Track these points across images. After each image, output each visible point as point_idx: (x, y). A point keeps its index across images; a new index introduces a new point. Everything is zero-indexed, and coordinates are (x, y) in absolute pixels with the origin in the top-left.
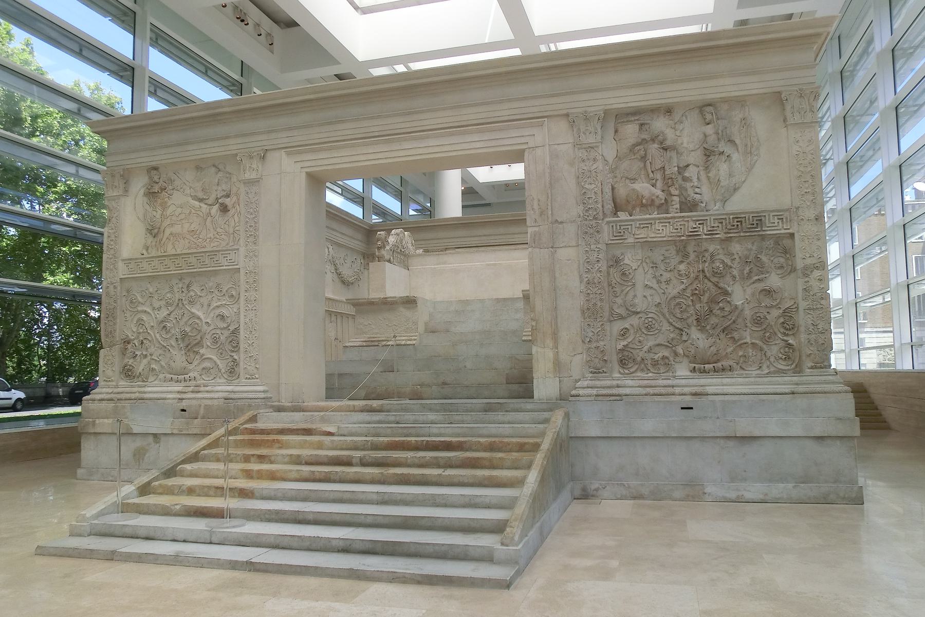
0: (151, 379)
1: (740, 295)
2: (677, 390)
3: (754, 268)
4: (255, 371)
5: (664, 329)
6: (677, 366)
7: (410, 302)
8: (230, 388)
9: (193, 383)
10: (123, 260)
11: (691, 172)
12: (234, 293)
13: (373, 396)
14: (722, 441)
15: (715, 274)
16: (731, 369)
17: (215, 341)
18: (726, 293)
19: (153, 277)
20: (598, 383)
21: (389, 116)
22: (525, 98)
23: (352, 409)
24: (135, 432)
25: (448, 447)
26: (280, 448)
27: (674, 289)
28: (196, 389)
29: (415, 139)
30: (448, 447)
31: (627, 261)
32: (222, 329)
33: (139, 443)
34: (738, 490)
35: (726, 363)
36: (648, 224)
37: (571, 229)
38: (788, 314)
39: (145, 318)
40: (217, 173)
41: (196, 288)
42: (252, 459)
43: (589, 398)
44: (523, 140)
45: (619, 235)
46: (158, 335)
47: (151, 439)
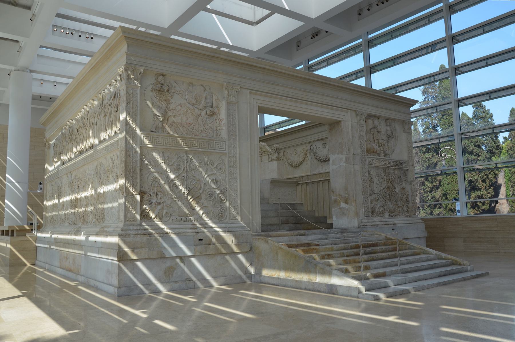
1: (397, 190)
2: (389, 223)
24: (167, 256)
33: (168, 263)
38: (407, 197)
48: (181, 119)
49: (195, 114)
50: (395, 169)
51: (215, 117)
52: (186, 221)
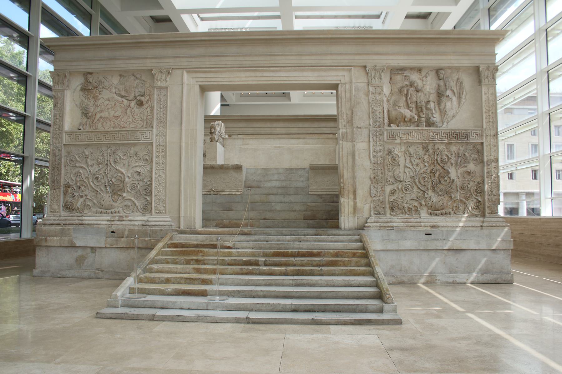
0: (86, 211)
2: (423, 224)
3: (461, 160)
4: (163, 208)
5: (414, 190)
6: (421, 211)
7: (238, 168)
8: (145, 219)
9: (118, 215)
10: (66, 132)
11: (432, 105)
12: (148, 158)
13: (221, 226)
14: (446, 252)
15: (442, 161)
16: (450, 214)
17: (133, 188)
18: (448, 172)
19: (88, 145)
20: (380, 220)
21: (256, 56)
22: (341, 54)
23: (231, 233)
25: (311, 255)
26: (203, 256)
27: (421, 169)
28: (121, 219)
29: (272, 71)
30: (311, 255)
31: (396, 152)
32: (138, 181)
33: (80, 252)
34: (453, 278)
35: (447, 211)
36: (409, 133)
37: (365, 132)
39: (81, 172)
40: (135, 80)
41: (120, 153)
42: (192, 262)
43: (376, 228)
44: (338, 78)
45: (392, 137)
46: (91, 183)
47: (89, 250)
48: (109, 113)
49: (123, 106)
50: (449, 144)
51: (146, 106)
52: (106, 213)
